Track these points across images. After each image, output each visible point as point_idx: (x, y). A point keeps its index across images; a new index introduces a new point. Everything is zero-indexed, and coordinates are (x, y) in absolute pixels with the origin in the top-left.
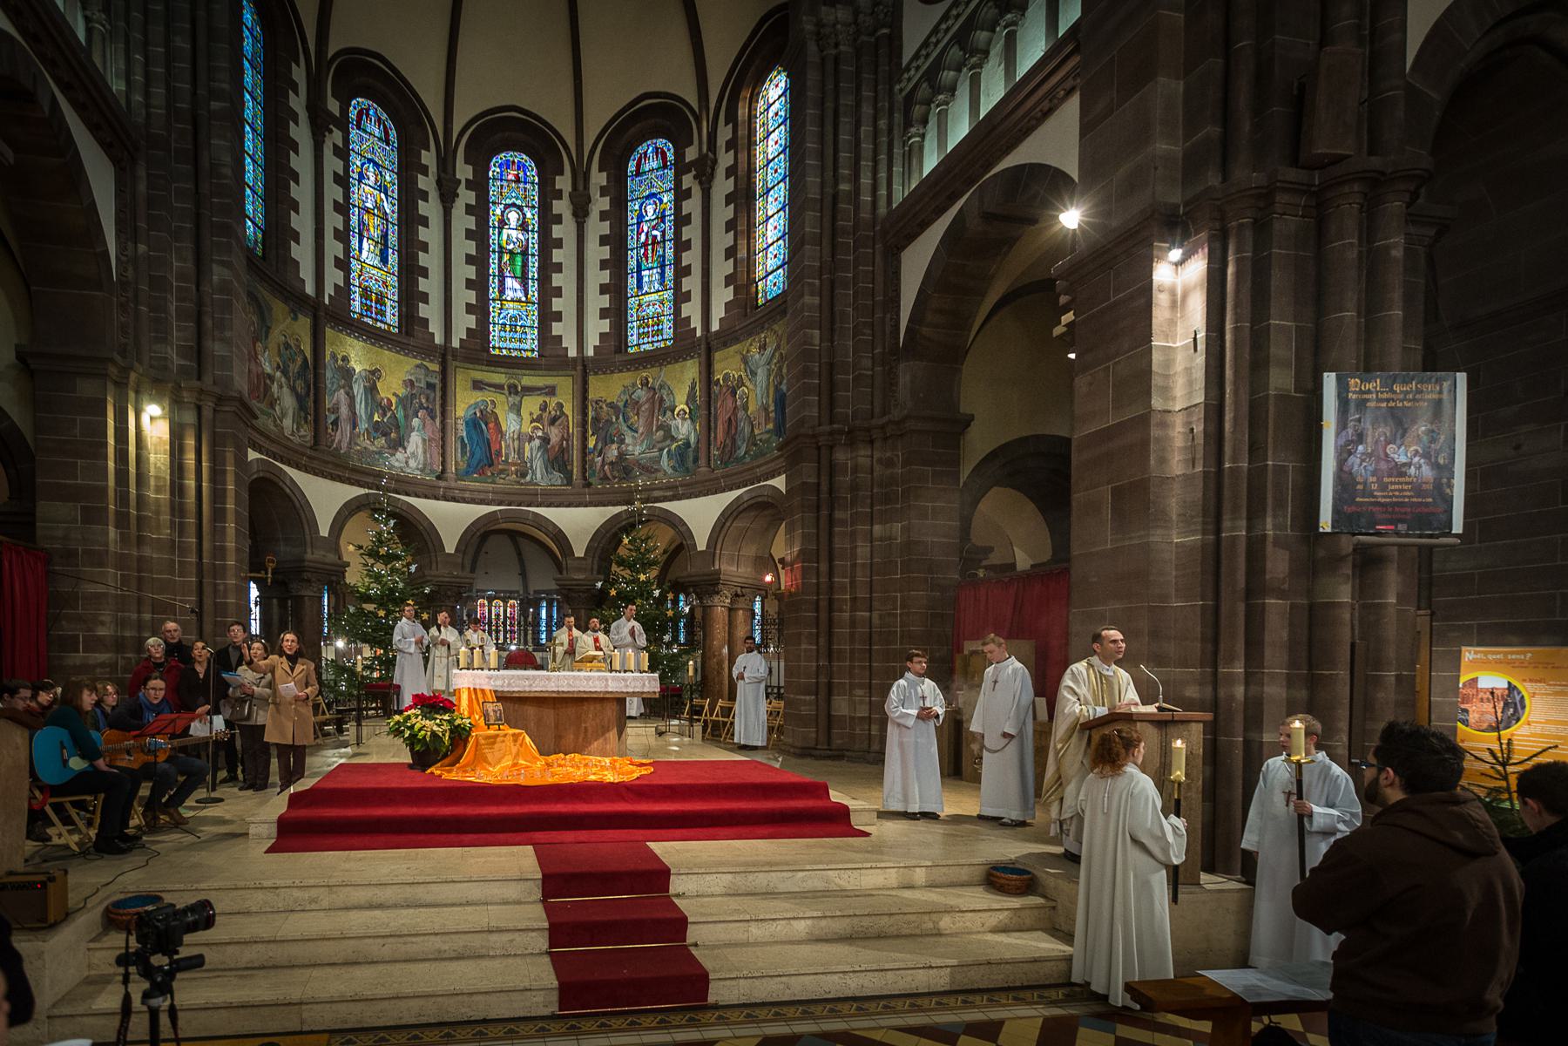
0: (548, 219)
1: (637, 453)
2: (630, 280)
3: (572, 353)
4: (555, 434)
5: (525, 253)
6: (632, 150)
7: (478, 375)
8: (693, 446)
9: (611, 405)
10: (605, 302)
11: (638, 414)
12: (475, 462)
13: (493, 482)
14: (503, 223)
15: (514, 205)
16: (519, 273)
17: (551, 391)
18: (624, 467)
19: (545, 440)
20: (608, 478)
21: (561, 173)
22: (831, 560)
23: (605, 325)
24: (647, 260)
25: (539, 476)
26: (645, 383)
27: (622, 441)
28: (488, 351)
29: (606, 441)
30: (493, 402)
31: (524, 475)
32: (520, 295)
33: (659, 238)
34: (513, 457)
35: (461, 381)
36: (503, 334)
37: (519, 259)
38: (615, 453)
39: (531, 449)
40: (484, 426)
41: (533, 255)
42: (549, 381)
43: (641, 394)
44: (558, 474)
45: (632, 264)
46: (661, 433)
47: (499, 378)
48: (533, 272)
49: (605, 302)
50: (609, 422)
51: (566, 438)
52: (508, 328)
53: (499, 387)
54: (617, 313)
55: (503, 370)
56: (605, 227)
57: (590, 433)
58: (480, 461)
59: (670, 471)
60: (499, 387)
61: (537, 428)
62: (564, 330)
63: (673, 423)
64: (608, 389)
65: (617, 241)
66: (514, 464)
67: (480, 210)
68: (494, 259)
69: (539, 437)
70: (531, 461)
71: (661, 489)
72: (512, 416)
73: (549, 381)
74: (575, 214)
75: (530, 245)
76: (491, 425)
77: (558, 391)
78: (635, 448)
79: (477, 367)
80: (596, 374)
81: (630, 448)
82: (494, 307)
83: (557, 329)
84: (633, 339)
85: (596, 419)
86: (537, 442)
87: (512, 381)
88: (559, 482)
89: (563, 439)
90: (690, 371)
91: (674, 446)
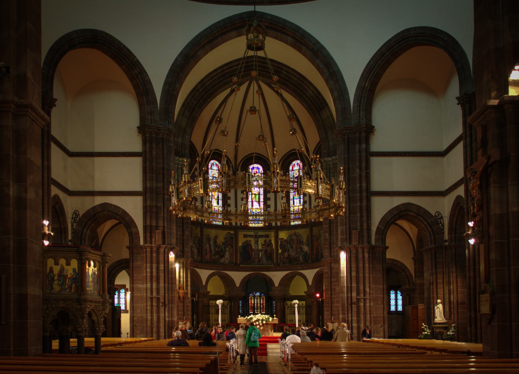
1: (293, 255)
2: (291, 202)
5: (259, 194)
6: (291, 163)
7: (245, 233)
8: (308, 254)
9: (286, 240)
13: (250, 265)
16: (257, 200)
19: (266, 251)
24: (296, 196)
25: (264, 262)
27: (289, 251)
30: (250, 241)
31: (259, 262)
32: (258, 207)
35: (241, 234)
37: (257, 196)
38: (287, 255)
39: (262, 254)
40: (247, 248)
41: (262, 194)
42: (267, 233)
43: (294, 237)
44: (270, 261)
45: (291, 197)
46: (299, 249)
47: (252, 233)
48: (262, 199)
53: (251, 236)
55: (253, 231)
57: (279, 249)
59: (302, 261)
60: (251, 236)
63: (303, 247)
69: (264, 250)
73: (267, 233)
75: (261, 192)
76: (249, 248)
78: (293, 254)
80: (281, 231)
81: (291, 253)
86: (263, 252)
87: (255, 234)
89: (271, 250)
91: (303, 254)
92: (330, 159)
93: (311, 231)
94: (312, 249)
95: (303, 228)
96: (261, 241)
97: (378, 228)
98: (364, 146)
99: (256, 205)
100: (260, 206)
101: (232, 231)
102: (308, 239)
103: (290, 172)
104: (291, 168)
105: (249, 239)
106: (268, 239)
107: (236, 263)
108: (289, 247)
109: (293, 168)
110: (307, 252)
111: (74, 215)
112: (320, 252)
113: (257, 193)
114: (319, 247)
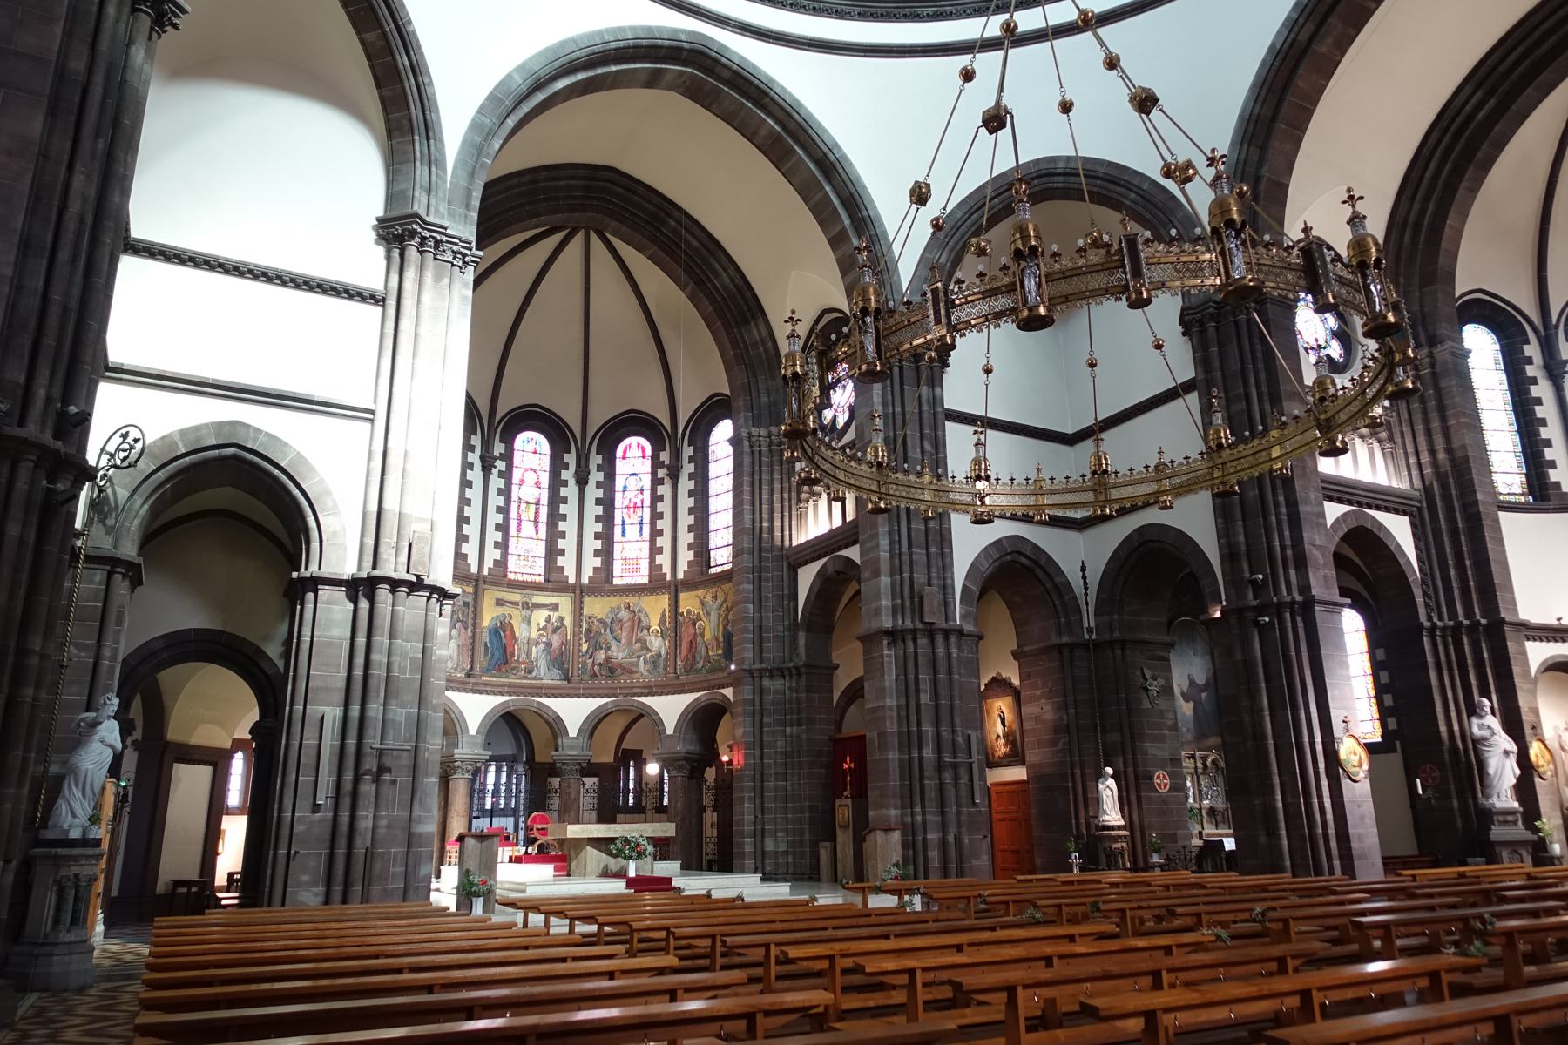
0: (556, 483)
1: (620, 658)
3: (572, 580)
4: (556, 640)
5: (537, 503)
9: (601, 621)
10: (598, 544)
11: (621, 629)
12: (493, 662)
13: (507, 677)
14: (522, 482)
15: (531, 469)
16: (533, 519)
17: (555, 607)
18: (610, 669)
19: (549, 645)
20: (596, 676)
21: (569, 452)
22: (762, 749)
23: (598, 562)
25: (542, 672)
26: (628, 607)
27: (609, 648)
28: (506, 576)
29: (596, 647)
31: (530, 672)
33: (639, 504)
34: (523, 658)
35: (489, 597)
36: (518, 562)
37: (533, 508)
38: (603, 656)
43: (624, 615)
45: (618, 520)
46: (639, 645)
47: (516, 596)
48: (543, 517)
49: (598, 544)
50: (598, 633)
51: (565, 643)
52: (522, 558)
53: (515, 604)
54: (606, 553)
56: (600, 493)
58: (499, 660)
59: (645, 673)
61: (542, 635)
62: (567, 563)
63: (648, 638)
64: (596, 607)
65: (608, 503)
66: (525, 663)
67: (507, 475)
68: (514, 507)
69: (544, 642)
70: (537, 660)
71: (639, 687)
72: (524, 626)
74: (578, 482)
76: (508, 633)
77: (560, 607)
78: (619, 654)
79: (500, 588)
80: (589, 596)
81: (615, 654)
82: (512, 542)
83: (560, 561)
84: (616, 573)
85: (589, 631)
86: (542, 646)
88: (558, 677)
90: (664, 601)
91: (648, 655)
92: (763, 432)
93: (675, 603)
94: (676, 645)
95: (652, 594)
96: (540, 617)
97: (965, 589)
98: (924, 390)
99: (528, 528)
100: (537, 533)
101: (468, 585)
102: (662, 622)
103: (617, 460)
104: (619, 452)
105: (506, 610)
106: (554, 615)
107: (471, 669)
108: (610, 638)
109: (625, 452)
110: (659, 655)
111: (117, 440)
112: (704, 651)
113: (533, 501)
114: (699, 639)
